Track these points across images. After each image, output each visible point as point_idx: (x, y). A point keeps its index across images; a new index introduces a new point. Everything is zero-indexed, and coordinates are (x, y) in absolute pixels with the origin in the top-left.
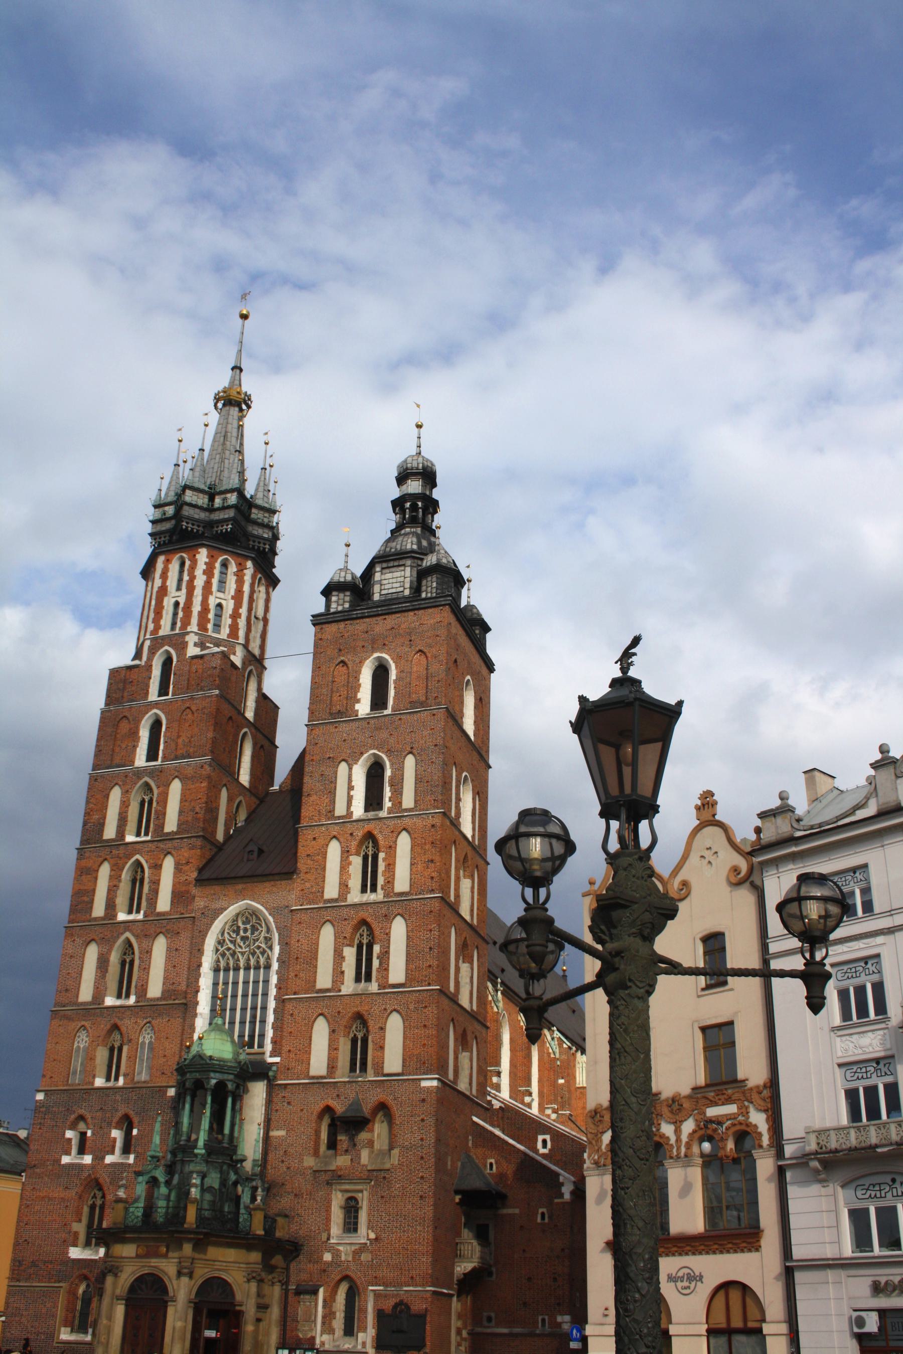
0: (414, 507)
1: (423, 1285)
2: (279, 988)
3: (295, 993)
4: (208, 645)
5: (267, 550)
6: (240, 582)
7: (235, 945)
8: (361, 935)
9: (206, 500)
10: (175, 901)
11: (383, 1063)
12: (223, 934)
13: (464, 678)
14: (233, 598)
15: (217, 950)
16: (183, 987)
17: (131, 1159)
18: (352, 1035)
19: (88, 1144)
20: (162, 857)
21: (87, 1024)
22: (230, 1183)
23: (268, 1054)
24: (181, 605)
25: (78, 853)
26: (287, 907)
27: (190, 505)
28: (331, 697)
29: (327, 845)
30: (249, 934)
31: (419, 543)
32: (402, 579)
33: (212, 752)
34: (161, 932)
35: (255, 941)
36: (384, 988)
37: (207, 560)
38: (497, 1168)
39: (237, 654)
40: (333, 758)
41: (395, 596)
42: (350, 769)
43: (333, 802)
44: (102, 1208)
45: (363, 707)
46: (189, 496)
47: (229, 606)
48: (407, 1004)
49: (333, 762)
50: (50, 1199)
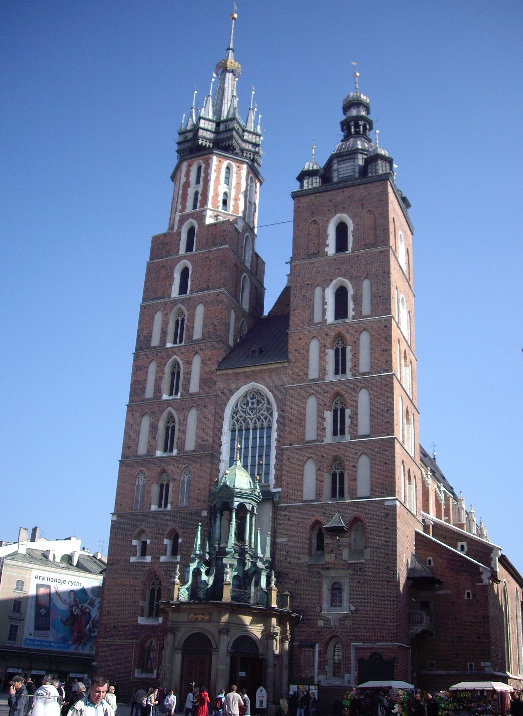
1: (391, 642)
2: (278, 441)
7: (245, 414)
9: (214, 125)
10: (203, 385)
11: (356, 490)
12: (237, 406)
15: (233, 417)
16: (210, 442)
17: (179, 557)
18: (332, 472)
19: (148, 548)
21: (144, 469)
23: (272, 486)
24: (200, 192)
25: (134, 356)
26: (283, 386)
27: (204, 129)
29: (309, 343)
30: (255, 406)
32: (353, 167)
34: (193, 406)
36: (355, 438)
38: (434, 563)
39: (238, 224)
40: (311, 284)
42: (324, 291)
43: (312, 313)
44: (159, 591)
45: (331, 249)
49: (311, 287)
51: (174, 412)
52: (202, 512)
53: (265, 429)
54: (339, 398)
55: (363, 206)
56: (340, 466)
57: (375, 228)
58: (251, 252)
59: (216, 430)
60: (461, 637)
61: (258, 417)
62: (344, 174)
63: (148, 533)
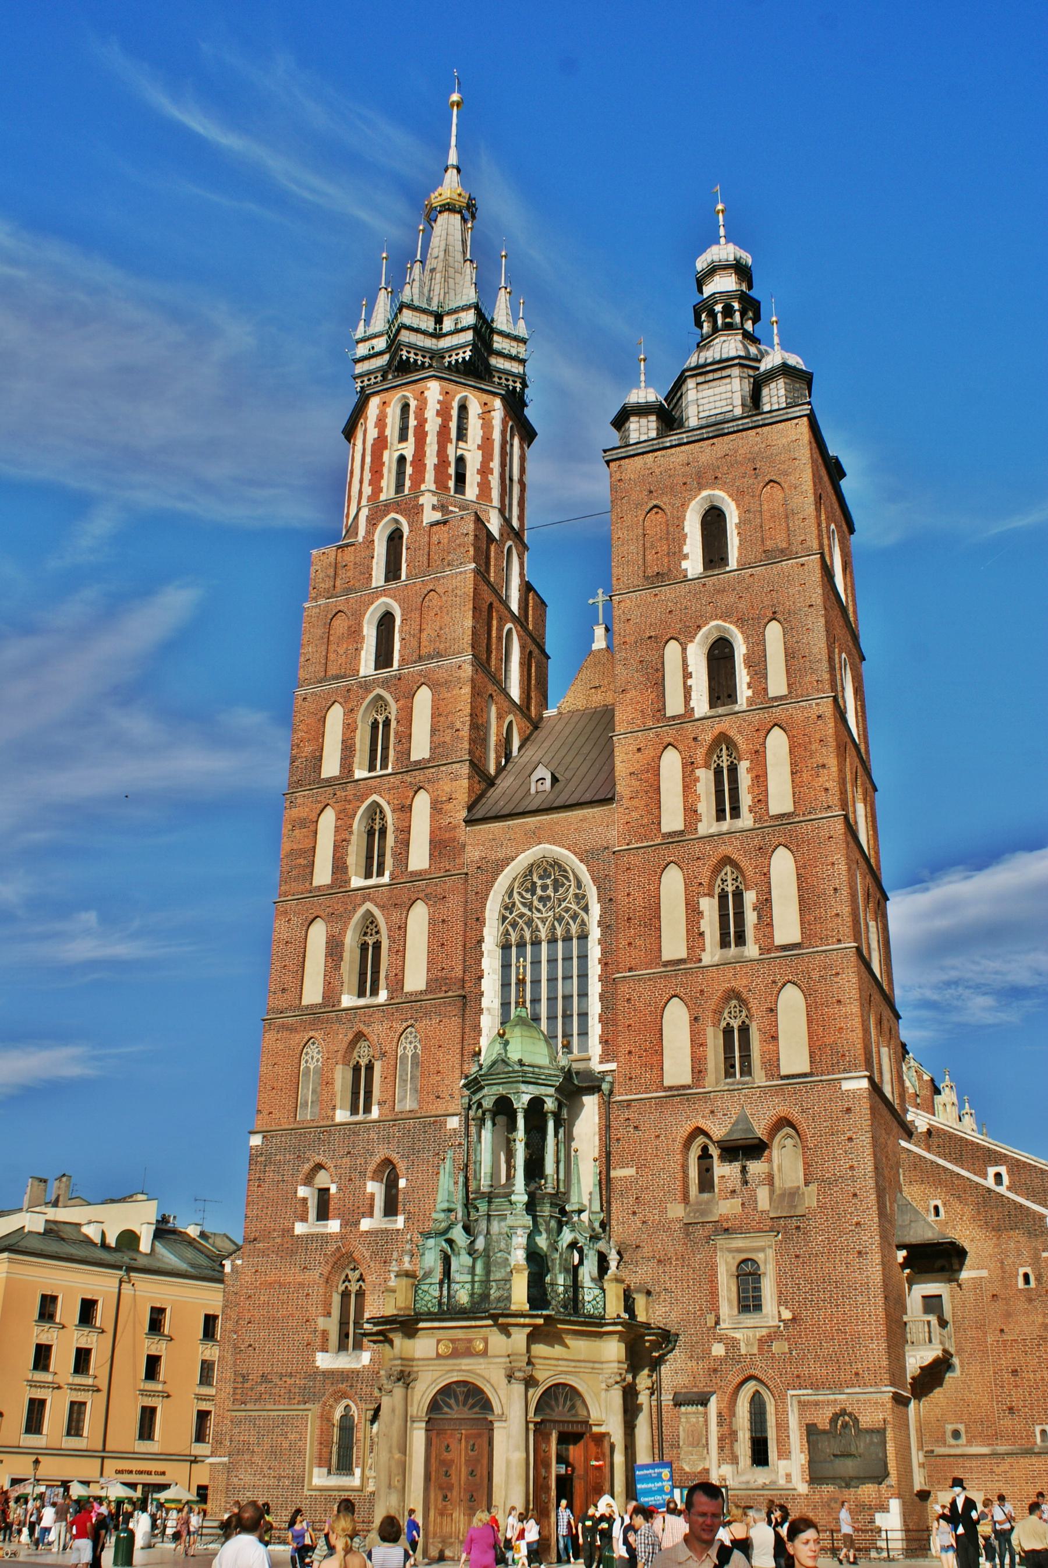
0: (728, 311)
2: (604, 964)
3: (630, 970)
4: (451, 508)
5: (518, 389)
7: (530, 910)
8: (723, 881)
10: (436, 854)
11: (778, 1060)
12: (511, 895)
14: (479, 447)
16: (458, 972)
17: (400, 1221)
18: (723, 1024)
19: (332, 1205)
20: (411, 794)
22: (565, 1246)
24: (409, 458)
26: (607, 848)
32: (729, 395)
34: (418, 899)
35: (560, 901)
36: (769, 951)
37: (441, 398)
39: (491, 521)
40: (656, 637)
42: (684, 650)
45: (693, 564)
48: (808, 973)
50: (281, 1285)
51: (376, 912)
52: (449, 1119)
53: (575, 941)
54: (728, 868)
56: (741, 1011)
57: (787, 517)
59: (468, 945)
60: (1016, 1371)
61: (557, 915)
63: (332, 1169)
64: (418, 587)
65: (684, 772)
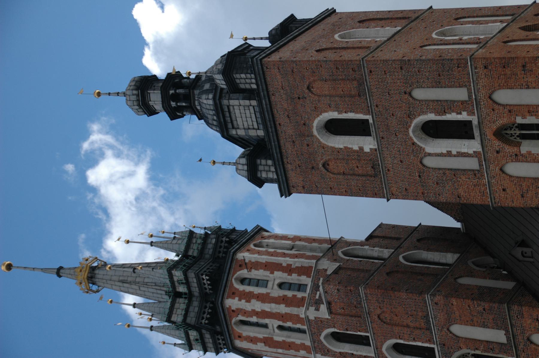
0: (176, 98)
4: (317, 297)
5: (227, 239)
6: (256, 265)
9: (181, 300)
13: (337, 40)
14: (272, 273)
20: (533, 346)
24: (281, 323)
27: (186, 316)
28: (359, 175)
29: (511, 176)
31: (207, 92)
32: (242, 108)
33: (421, 293)
37: (237, 298)
39: (326, 268)
40: (419, 172)
41: (258, 115)
42: (430, 155)
43: (464, 171)
46: (178, 317)
47: (280, 276)
49: (424, 172)
55: (301, 97)
57: (334, 80)
58: (366, 247)
62: (252, 121)
64: (376, 326)
65: (523, 161)
